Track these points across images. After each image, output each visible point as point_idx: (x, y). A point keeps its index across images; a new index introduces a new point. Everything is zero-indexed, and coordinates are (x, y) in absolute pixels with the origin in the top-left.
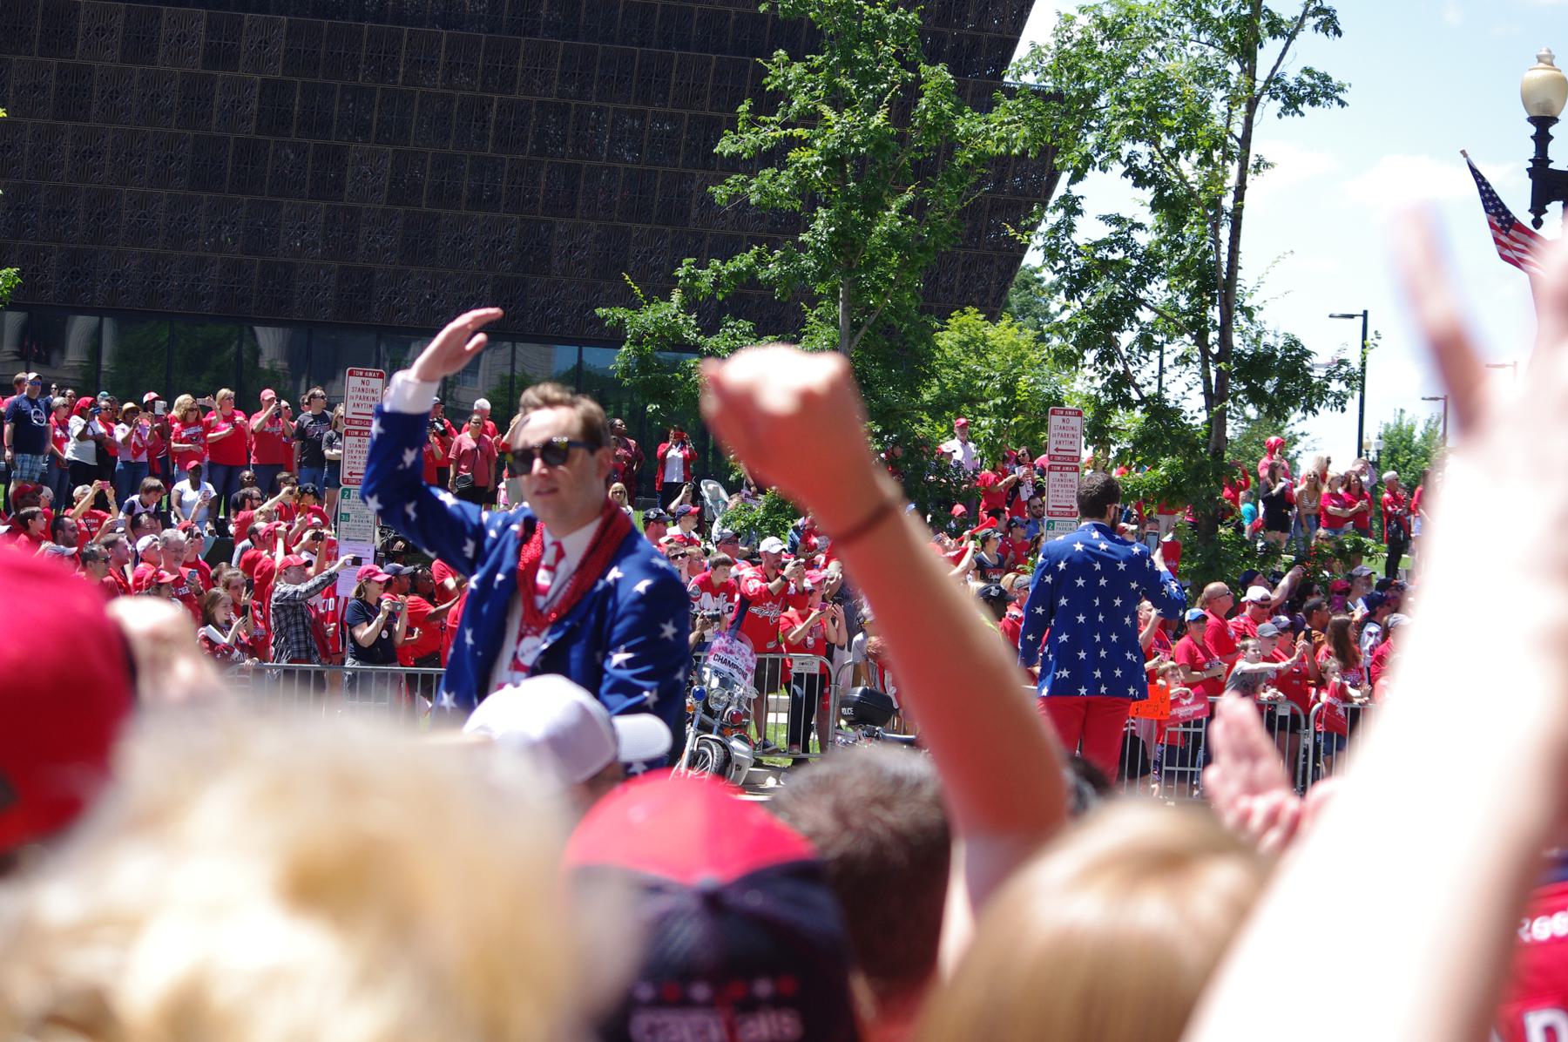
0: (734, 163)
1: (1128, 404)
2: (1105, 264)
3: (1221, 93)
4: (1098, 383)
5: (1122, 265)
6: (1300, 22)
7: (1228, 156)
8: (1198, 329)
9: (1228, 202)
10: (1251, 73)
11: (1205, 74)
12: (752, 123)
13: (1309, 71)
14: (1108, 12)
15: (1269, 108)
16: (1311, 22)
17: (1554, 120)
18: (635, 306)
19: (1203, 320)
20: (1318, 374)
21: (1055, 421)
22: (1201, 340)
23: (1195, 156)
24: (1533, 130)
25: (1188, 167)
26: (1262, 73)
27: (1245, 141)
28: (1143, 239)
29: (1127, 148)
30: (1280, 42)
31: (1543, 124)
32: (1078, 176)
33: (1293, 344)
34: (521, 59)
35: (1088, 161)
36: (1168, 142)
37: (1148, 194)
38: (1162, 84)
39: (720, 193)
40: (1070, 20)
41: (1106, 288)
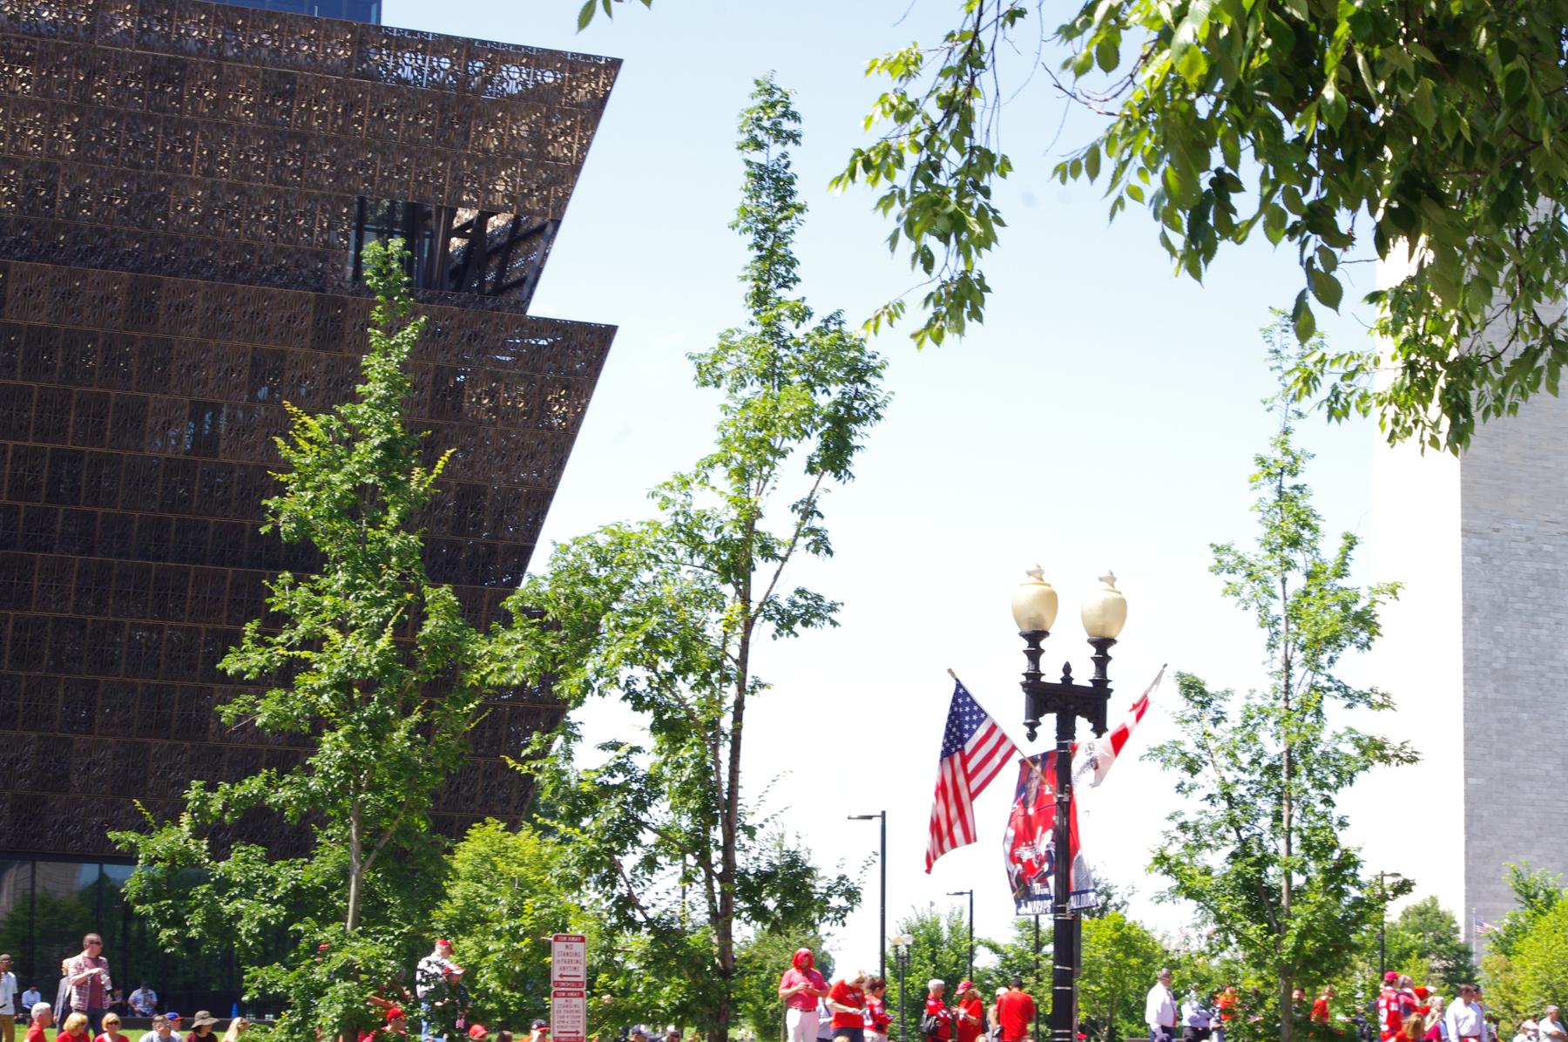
0: (238, 684)
1: (636, 927)
2: (606, 791)
3: (714, 615)
4: (606, 904)
5: (622, 788)
7: (726, 678)
8: (699, 845)
9: (726, 723)
12: (260, 642)
13: (801, 592)
14: (603, 540)
15: (764, 629)
16: (802, 541)
17: (1044, 634)
18: (144, 829)
19: (706, 841)
20: (820, 887)
21: (558, 947)
22: (704, 860)
23: (692, 678)
25: (683, 687)
26: (757, 596)
27: (743, 661)
28: (644, 763)
29: (625, 673)
30: (773, 565)
31: (1035, 638)
32: (579, 702)
33: (794, 861)
34: (36, 576)
35: (587, 686)
36: (665, 666)
37: (648, 717)
38: (654, 604)
39: (228, 712)
41: (610, 811)
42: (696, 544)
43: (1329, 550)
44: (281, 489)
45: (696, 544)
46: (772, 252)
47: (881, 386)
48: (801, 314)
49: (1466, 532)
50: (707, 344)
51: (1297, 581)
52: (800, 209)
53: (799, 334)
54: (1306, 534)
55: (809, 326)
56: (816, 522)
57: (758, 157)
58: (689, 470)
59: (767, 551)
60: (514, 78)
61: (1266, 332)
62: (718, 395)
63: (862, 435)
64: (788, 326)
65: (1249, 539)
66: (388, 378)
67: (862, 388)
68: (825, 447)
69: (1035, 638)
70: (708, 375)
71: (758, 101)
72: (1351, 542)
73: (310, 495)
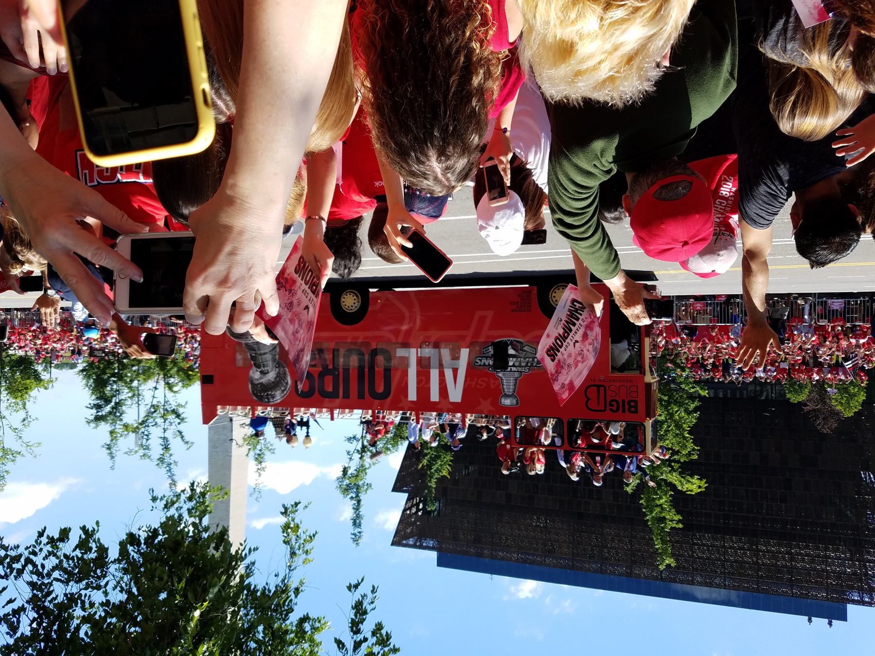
6: (354, 453)
10: (363, 442)
13: (352, 443)
14: (389, 452)
15: (359, 436)
24: (309, 434)
31: (307, 436)
40: (396, 451)
43: (252, 453)
44: (451, 461)
48: (352, 498)
49: (231, 456)
50: (369, 491)
51: (259, 447)
52: (351, 519)
53: (352, 494)
54: (256, 456)
55: (350, 496)
56: (349, 457)
57: (359, 530)
59: (358, 451)
60: (411, 541)
61: (261, 497)
63: (340, 474)
64: (354, 495)
65: (268, 455)
66: (431, 482)
68: (347, 471)
69: (307, 436)
70: (369, 486)
71: (359, 541)
73: (445, 459)
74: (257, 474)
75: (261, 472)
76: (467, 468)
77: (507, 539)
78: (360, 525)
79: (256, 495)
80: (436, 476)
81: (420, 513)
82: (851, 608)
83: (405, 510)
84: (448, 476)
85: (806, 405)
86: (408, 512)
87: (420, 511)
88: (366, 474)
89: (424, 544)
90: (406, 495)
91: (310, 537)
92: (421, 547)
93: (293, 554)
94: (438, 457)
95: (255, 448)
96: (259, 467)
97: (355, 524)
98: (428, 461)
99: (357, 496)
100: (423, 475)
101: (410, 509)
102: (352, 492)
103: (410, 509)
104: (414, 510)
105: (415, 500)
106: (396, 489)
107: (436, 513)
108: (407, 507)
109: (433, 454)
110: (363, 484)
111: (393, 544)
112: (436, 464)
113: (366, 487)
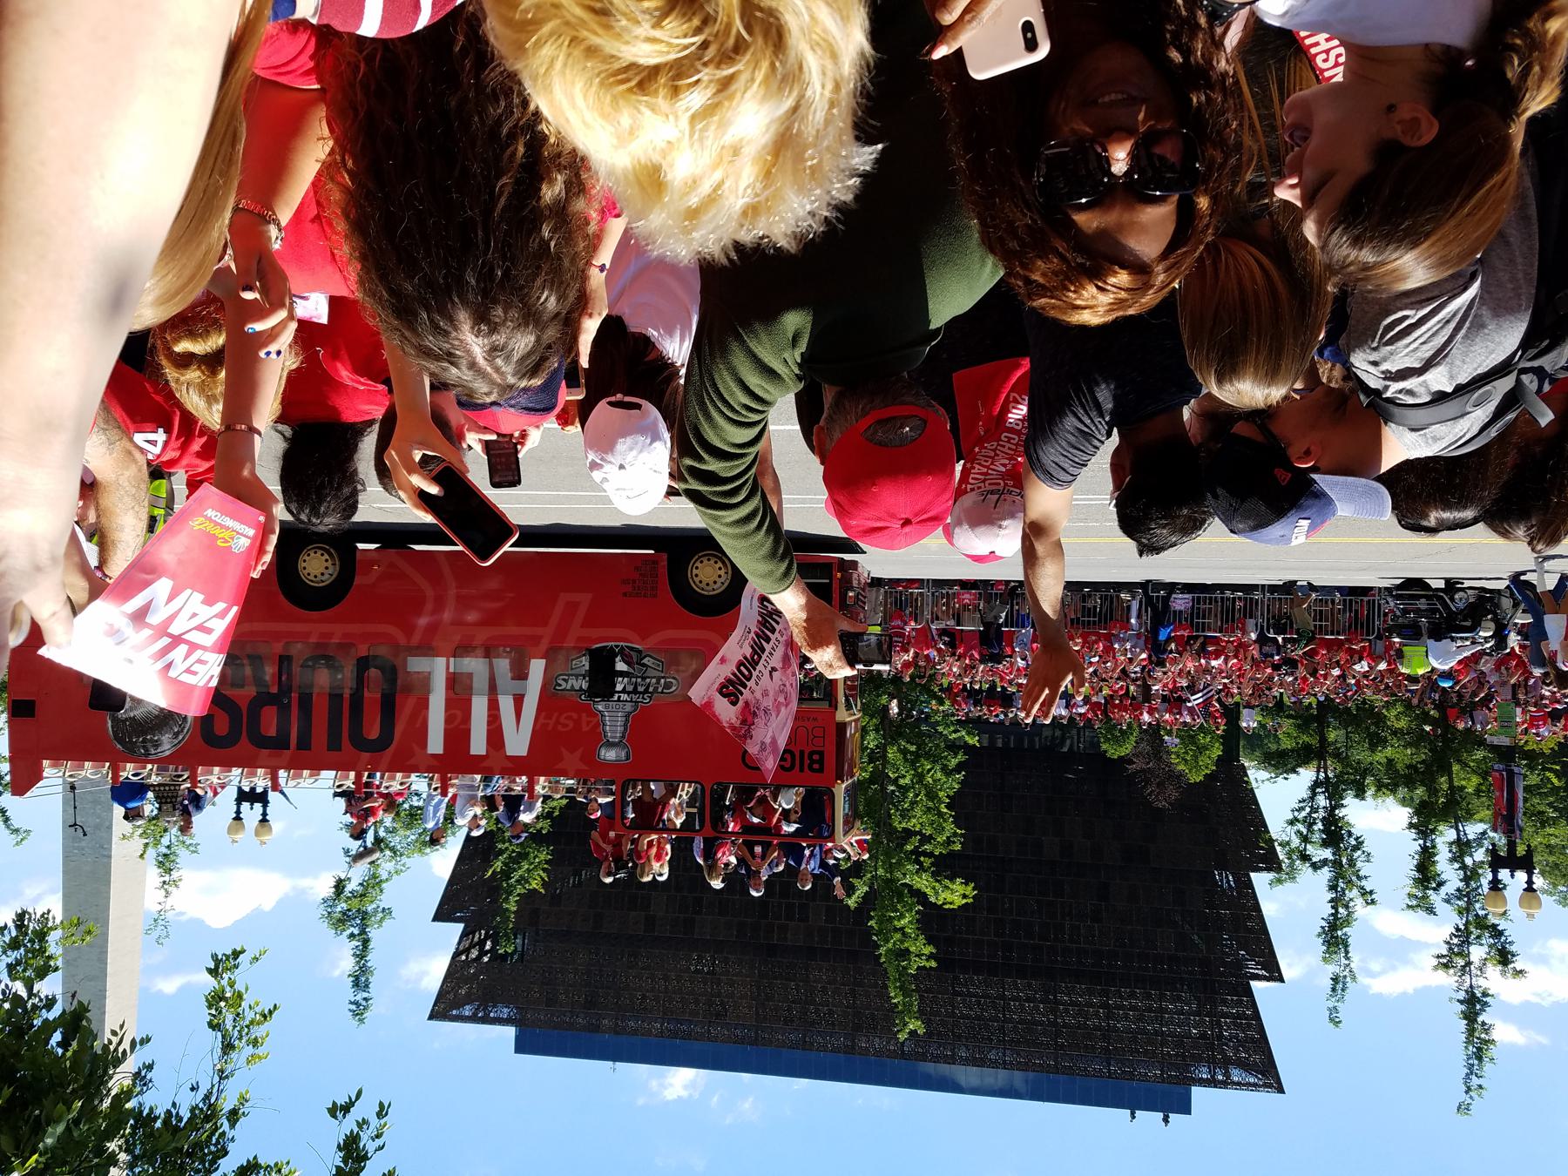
3: (388, 824)
11: (393, 831)
12: (554, 808)
17: (261, 821)
42: (393, 850)
43: (151, 852)
44: (547, 862)
45: (393, 850)
46: (361, 959)
47: (322, 911)
48: (352, 936)
51: (165, 841)
52: (350, 975)
53: (352, 929)
54: (160, 859)
57: (365, 995)
58: (395, 877)
60: (467, 1011)
62: (382, 905)
64: (356, 931)
66: (508, 903)
67: (329, 910)
68: (344, 887)
70: (387, 912)
71: (364, 1016)
72: (142, 856)
73: (537, 860)
74: (163, 892)
75: (170, 889)
76: (577, 873)
77: (644, 997)
78: (367, 986)
79: (159, 931)
80: (519, 890)
81: (486, 959)
82: (1196, 1092)
83: (457, 954)
84: (542, 891)
85: (1131, 762)
86: (464, 957)
87: (486, 955)
88: (381, 891)
89: (492, 1015)
90: (460, 927)
91: (265, 1016)
92: (486, 1020)
93: (228, 1047)
94: (523, 856)
95: (157, 843)
96: (167, 878)
97: (356, 984)
98: (505, 864)
99: (363, 932)
100: (495, 889)
101: (467, 951)
102: (352, 926)
103: (467, 951)
104: (474, 953)
105: (477, 936)
106: (442, 915)
107: (516, 957)
108: (461, 948)
109: (513, 851)
110: (376, 911)
111: (431, 1018)
112: (520, 868)
113: (381, 915)
